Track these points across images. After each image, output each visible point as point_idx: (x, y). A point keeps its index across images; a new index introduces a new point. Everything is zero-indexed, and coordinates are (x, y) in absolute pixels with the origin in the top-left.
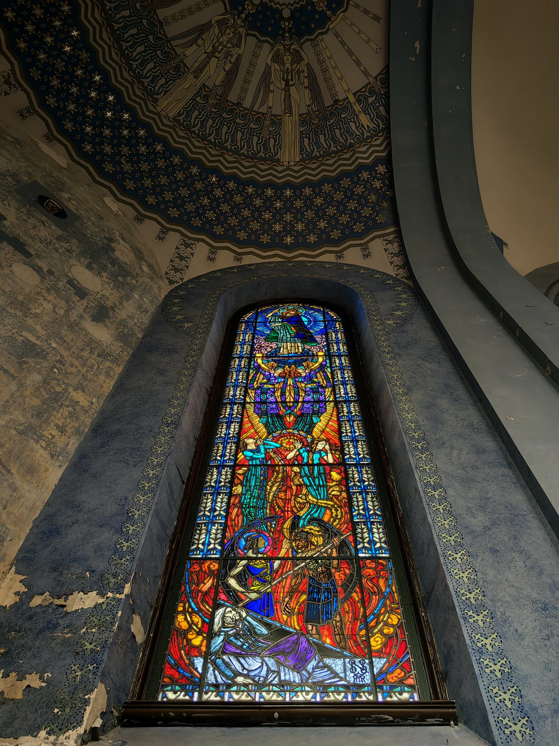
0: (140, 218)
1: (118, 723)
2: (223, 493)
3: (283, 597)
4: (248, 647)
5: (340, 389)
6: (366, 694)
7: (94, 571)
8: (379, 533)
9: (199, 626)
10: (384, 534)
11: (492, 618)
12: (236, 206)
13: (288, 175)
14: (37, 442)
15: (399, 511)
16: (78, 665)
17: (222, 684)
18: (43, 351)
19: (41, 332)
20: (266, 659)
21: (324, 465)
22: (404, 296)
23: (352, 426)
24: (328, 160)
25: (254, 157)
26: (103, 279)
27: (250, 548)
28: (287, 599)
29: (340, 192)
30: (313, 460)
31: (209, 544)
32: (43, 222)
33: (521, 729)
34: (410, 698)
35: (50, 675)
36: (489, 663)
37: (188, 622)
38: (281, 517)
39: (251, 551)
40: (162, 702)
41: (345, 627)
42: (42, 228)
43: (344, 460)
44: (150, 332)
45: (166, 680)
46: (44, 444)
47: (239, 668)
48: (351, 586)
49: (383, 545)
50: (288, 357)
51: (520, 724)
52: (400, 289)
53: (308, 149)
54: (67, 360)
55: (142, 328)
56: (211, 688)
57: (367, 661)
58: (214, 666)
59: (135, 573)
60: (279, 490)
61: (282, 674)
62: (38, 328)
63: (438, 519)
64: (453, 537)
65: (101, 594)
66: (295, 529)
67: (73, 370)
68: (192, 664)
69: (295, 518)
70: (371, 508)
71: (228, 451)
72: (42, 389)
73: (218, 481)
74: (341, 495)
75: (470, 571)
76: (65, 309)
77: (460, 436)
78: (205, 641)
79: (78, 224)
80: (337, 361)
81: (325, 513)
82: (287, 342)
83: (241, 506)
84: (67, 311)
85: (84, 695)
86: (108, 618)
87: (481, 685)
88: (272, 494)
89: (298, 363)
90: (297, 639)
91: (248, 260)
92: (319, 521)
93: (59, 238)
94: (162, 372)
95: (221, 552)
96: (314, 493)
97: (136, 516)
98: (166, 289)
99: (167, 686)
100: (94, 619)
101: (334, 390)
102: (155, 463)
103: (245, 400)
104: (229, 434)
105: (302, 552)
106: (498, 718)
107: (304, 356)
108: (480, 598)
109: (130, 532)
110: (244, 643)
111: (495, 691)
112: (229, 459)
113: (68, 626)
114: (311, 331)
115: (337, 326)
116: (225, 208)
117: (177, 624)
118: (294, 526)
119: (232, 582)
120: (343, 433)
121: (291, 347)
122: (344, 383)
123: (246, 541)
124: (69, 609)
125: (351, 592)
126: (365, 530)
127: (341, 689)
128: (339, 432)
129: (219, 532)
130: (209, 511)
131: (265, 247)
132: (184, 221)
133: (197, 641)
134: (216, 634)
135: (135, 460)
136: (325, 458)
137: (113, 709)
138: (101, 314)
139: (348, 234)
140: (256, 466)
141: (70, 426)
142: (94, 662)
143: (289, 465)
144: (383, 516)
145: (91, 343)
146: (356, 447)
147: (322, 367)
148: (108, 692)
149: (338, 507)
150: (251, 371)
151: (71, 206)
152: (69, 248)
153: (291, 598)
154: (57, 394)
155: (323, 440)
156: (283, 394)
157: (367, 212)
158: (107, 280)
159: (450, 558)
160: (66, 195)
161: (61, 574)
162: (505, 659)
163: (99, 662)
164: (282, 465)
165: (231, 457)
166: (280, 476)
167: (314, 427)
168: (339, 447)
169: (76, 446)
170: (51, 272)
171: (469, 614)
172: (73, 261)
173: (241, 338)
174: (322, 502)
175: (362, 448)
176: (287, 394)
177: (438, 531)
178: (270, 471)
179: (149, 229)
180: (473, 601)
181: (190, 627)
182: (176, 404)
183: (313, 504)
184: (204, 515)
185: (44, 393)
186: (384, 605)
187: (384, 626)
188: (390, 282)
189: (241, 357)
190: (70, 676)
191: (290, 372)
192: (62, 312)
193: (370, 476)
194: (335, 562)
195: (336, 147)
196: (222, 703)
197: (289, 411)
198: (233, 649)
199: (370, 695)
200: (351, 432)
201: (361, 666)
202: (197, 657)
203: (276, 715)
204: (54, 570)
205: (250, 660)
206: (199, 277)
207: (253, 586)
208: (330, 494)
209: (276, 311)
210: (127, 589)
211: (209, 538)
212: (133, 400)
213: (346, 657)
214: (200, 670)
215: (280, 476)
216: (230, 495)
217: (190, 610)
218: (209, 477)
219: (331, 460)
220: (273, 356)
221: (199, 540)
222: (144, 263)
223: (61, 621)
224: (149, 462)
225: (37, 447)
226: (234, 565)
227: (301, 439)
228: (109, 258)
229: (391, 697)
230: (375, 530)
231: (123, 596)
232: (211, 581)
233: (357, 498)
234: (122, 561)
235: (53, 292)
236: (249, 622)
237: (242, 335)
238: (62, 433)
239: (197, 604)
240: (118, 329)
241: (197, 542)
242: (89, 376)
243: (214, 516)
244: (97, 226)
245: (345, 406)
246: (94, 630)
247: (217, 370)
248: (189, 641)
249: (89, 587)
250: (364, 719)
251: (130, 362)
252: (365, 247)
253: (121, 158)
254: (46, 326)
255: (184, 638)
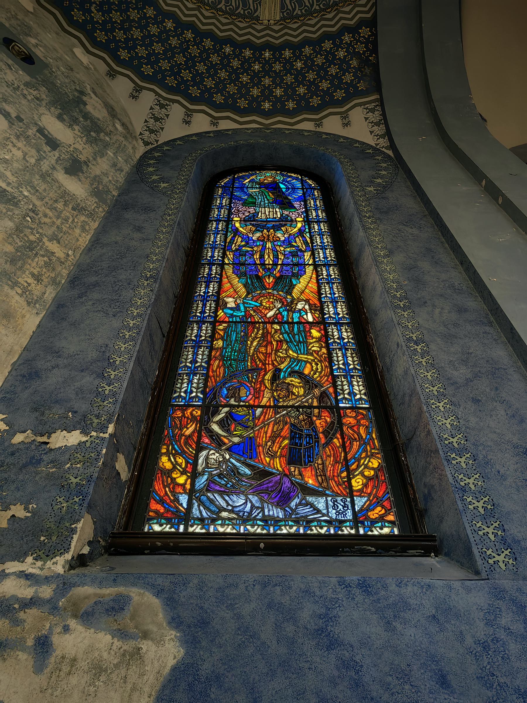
0: (112, 74)
1: (106, 552)
2: (204, 346)
3: (265, 442)
4: (232, 486)
5: (319, 254)
6: (348, 528)
7: (76, 412)
8: (359, 386)
9: (183, 466)
10: (364, 387)
11: (475, 460)
12: (213, 66)
13: (268, 35)
14: (12, 288)
15: (379, 366)
16: (64, 497)
17: (207, 518)
18: (14, 198)
19: (12, 179)
20: (250, 497)
21: (304, 323)
22: (384, 165)
23: (331, 288)
24: (310, 19)
25: (232, 13)
26: (75, 132)
27: (232, 397)
28: (269, 444)
29: (321, 55)
30: (292, 318)
31: (191, 392)
32: (9, 65)
33: (505, 559)
34: (391, 532)
35: (35, 506)
36: (472, 500)
37: (172, 463)
38: (262, 369)
39: (233, 399)
40: (148, 533)
41: (327, 469)
42: (8, 71)
43: (324, 319)
44: (124, 192)
45: (151, 514)
46: (20, 291)
47: (224, 504)
48: (332, 433)
49: (363, 397)
50: (267, 221)
51: (503, 555)
52: (380, 158)
53: (290, 7)
54: (41, 210)
55: (117, 187)
56: (196, 522)
57: (349, 500)
58: (199, 502)
59: (119, 415)
60: (259, 345)
61: (266, 511)
62: (8, 174)
63: (420, 371)
64: (436, 388)
65: (84, 432)
66: (276, 380)
67: (47, 220)
68: (177, 500)
69: (276, 371)
70: (351, 363)
71: (208, 308)
72: (15, 236)
73: (198, 336)
74: (321, 350)
75: (453, 418)
76: (36, 158)
77: (441, 296)
78: (189, 480)
79: (46, 72)
80: (316, 227)
81: (305, 367)
82: (265, 208)
83: (222, 358)
84: (39, 160)
85: (71, 525)
86: (92, 455)
87: (465, 519)
88: (253, 348)
89: (277, 228)
90: (280, 479)
91: (225, 125)
92: (300, 374)
93: (27, 84)
94: (139, 229)
95: (204, 400)
96: (294, 349)
97: (117, 363)
98: (142, 149)
99: (152, 519)
100: (79, 456)
101: (313, 255)
102: (135, 314)
103: (223, 261)
104: (209, 292)
105: (284, 401)
106: (482, 549)
107: (282, 221)
108: (462, 442)
109: (112, 377)
110: (227, 482)
111: (479, 525)
112: (209, 316)
113: (52, 462)
114: (290, 198)
115: (316, 193)
116: (201, 68)
117: (161, 464)
118: (275, 377)
119: (215, 428)
120: (323, 294)
121: (269, 212)
122: (323, 248)
123: (228, 390)
124: (52, 446)
125: (332, 439)
126: (345, 383)
127: (323, 524)
128: (319, 293)
129: (200, 381)
130: (191, 363)
131: (243, 112)
132: (157, 79)
133: (181, 480)
134: (200, 474)
135: (114, 310)
136: (305, 317)
137: (99, 539)
138: (75, 168)
139: (329, 102)
140: (236, 322)
141: (46, 276)
142: (79, 494)
143: (269, 323)
144: (363, 370)
145: (65, 196)
146: (335, 308)
147: (301, 232)
148: (95, 523)
149: (318, 361)
150: (229, 234)
151: (39, 52)
152: (38, 96)
153: (273, 443)
154: (32, 242)
155: (303, 300)
156: (262, 257)
157: (348, 78)
158: (79, 134)
159: (433, 406)
160: (33, 41)
161: (43, 414)
162: (488, 497)
163: (84, 495)
164: (262, 322)
165: (211, 314)
166: (261, 332)
167: (294, 288)
168: (319, 308)
169: (53, 295)
170: (19, 119)
171: (452, 456)
172: (42, 110)
173: (218, 202)
174: (303, 357)
175: (342, 309)
176: (266, 257)
177: (421, 382)
178: (250, 328)
179: (122, 86)
180: (456, 445)
181: (174, 468)
182: (154, 259)
183: (294, 358)
184: (186, 366)
185: (18, 241)
186: (365, 450)
187: (364, 468)
188: (370, 151)
189: (218, 221)
190: (56, 508)
191: (268, 236)
192: (33, 161)
193: (349, 334)
194: (316, 411)
195: (319, 5)
196: (208, 534)
197: (268, 273)
198: (218, 488)
199: (352, 529)
200: (330, 294)
201: (342, 504)
202: (181, 494)
203: (262, 545)
204: (36, 410)
205: (234, 498)
206: (175, 140)
207: (236, 431)
208: (310, 349)
209: (253, 177)
210: (111, 429)
211: (191, 387)
212: (110, 254)
213: (328, 495)
214: (185, 505)
215: (261, 332)
216: (211, 348)
217: (174, 452)
218: (190, 332)
219: (310, 319)
220: (250, 220)
221: (181, 388)
222: (118, 121)
223: (44, 457)
224: (129, 312)
225: (12, 293)
226: (216, 412)
227: (281, 299)
228: (81, 111)
229: (372, 531)
230: (355, 383)
231: (107, 435)
232: (194, 426)
233: (337, 353)
234: (105, 403)
235: (23, 139)
236: (232, 463)
237: (219, 199)
238: (38, 282)
239: (180, 447)
240: (93, 184)
241: (179, 390)
242: (64, 229)
243: (195, 367)
244: (67, 77)
245: (324, 269)
246: (78, 466)
247: (194, 231)
248: (173, 480)
249: (72, 427)
250: (347, 549)
251: (105, 218)
252: (344, 116)
253: (91, 6)
254: (16, 173)
255: (169, 477)
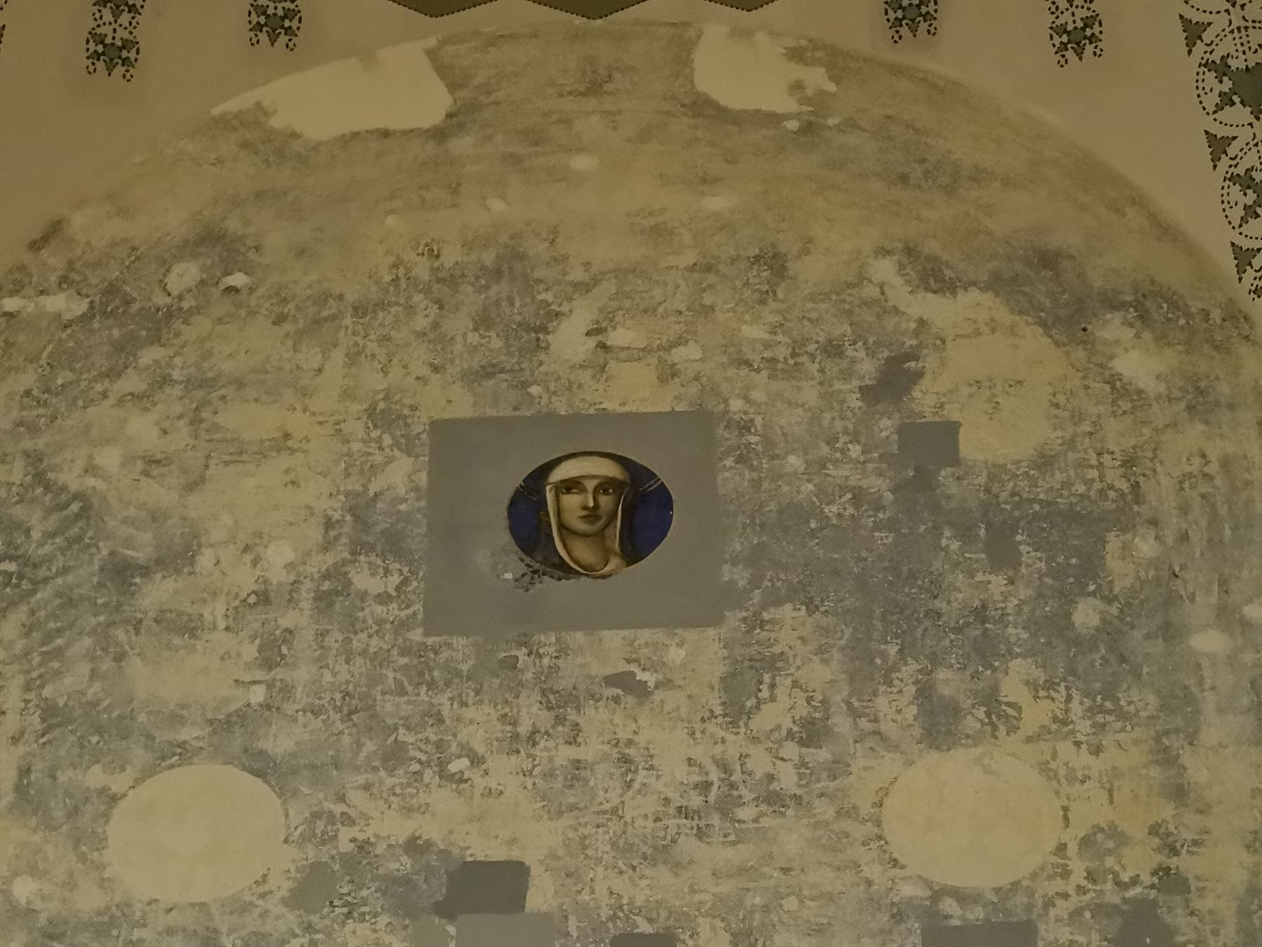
152: (802, 710)
